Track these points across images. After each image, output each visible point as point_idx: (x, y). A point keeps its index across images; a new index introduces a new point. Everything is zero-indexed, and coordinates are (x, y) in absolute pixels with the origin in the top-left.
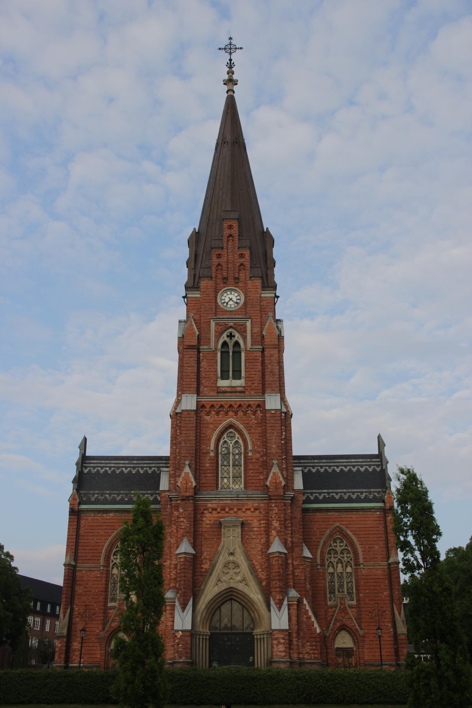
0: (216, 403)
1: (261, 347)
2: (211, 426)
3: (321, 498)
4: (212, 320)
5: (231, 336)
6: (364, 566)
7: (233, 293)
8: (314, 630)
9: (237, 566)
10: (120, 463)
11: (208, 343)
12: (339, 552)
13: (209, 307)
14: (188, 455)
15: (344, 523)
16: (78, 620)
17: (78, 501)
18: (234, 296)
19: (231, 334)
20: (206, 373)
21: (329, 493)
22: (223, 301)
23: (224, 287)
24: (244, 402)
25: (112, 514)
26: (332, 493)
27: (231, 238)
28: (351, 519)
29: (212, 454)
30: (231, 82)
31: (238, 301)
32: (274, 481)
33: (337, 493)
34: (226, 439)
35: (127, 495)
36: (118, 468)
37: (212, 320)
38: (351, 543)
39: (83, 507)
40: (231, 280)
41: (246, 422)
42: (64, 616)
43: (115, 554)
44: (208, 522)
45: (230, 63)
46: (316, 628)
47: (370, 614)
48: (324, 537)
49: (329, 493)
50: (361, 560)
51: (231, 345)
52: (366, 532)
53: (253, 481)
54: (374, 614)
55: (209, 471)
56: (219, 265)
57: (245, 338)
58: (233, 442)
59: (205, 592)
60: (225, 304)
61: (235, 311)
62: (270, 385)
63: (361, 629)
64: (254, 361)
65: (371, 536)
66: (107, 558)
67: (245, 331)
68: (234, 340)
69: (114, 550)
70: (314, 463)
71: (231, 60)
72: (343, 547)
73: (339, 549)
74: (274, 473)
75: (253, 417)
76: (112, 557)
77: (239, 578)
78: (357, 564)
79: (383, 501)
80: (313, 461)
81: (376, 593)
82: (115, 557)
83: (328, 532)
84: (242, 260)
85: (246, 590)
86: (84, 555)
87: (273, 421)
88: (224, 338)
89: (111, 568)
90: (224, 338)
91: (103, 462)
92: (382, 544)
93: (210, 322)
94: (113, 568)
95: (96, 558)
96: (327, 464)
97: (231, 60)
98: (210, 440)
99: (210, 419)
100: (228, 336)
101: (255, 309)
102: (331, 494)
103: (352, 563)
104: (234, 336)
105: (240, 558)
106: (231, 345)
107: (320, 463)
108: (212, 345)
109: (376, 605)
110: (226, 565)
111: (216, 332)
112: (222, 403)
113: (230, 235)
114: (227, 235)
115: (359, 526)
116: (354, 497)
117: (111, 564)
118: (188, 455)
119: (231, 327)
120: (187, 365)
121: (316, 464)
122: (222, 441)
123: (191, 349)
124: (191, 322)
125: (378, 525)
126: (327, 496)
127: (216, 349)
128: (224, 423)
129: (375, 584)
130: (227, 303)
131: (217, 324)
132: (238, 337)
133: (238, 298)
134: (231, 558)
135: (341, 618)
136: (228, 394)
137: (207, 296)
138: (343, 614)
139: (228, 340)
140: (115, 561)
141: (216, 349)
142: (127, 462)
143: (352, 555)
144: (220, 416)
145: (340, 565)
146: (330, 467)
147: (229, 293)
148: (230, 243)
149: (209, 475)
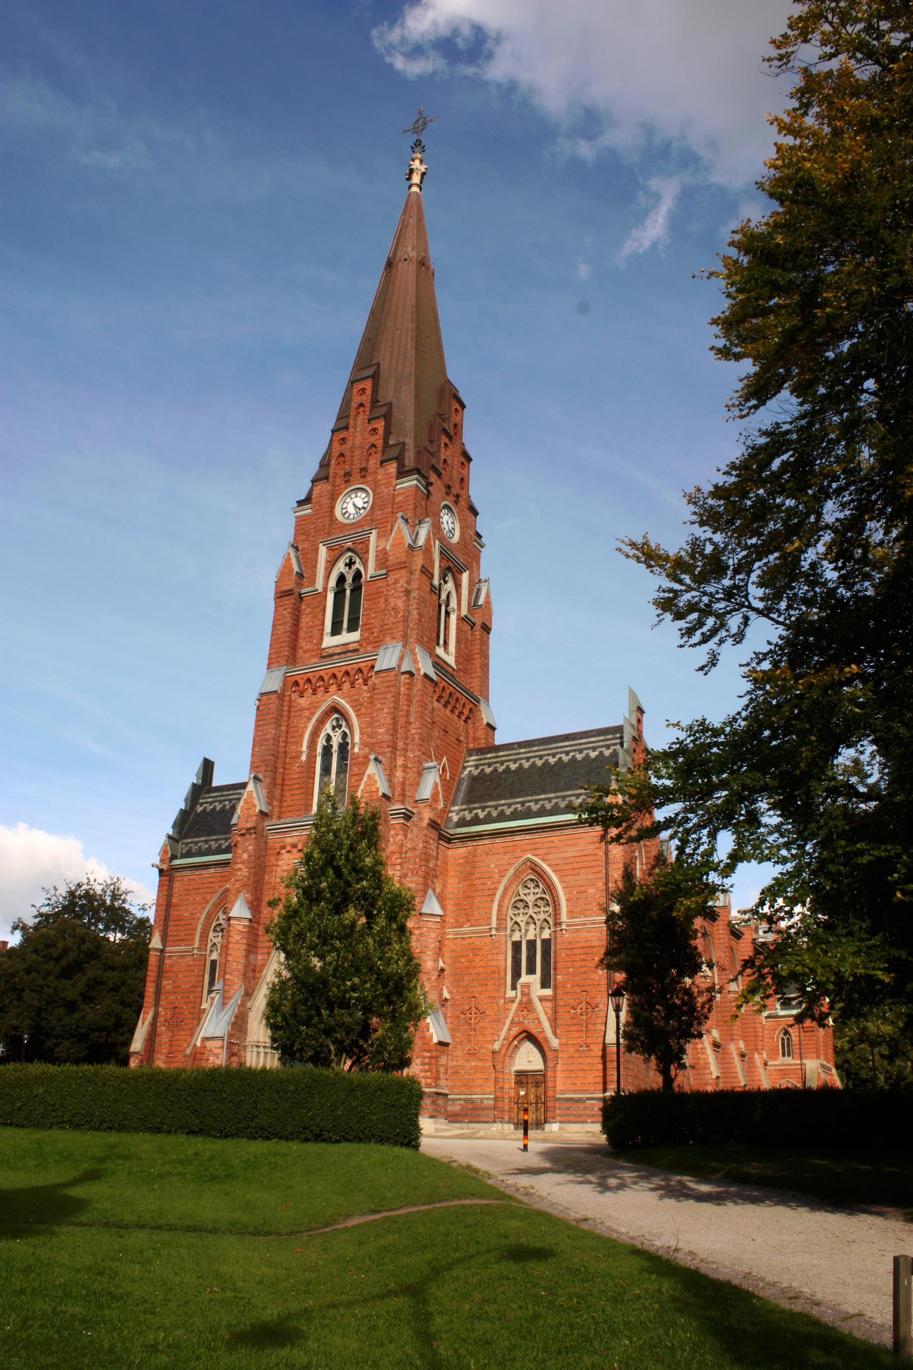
0: (313, 674)
3: (508, 812)
4: (321, 545)
6: (567, 926)
7: (359, 494)
8: (428, 1037)
11: (313, 582)
12: (530, 904)
14: (262, 764)
16: (164, 1028)
17: (169, 855)
18: (360, 500)
19: (351, 560)
22: (344, 511)
23: (346, 488)
24: (352, 666)
25: (212, 870)
26: (530, 801)
27: (362, 409)
28: (551, 844)
29: (304, 758)
32: (368, 788)
33: (536, 801)
34: (330, 732)
37: (321, 545)
38: (550, 888)
40: (356, 475)
42: (143, 1023)
43: (215, 930)
44: (285, 867)
46: (432, 1034)
47: (572, 1011)
48: (505, 881)
49: (523, 803)
50: (564, 917)
52: (575, 866)
54: (579, 1011)
55: (297, 786)
56: (342, 455)
61: (359, 522)
63: (555, 1034)
64: (376, 596)
66: (204, 936)
68: (354, 567)
69: (214, 924)
70: (520, 753)
72: (539, 896)
73: (530, 899)
74: (369, 776)
75: (365, 688)
78: (557, 923)
81: (585, 973)
83: (511, 871)
84: (373, 439)
86: (176, 933)
87: (382, 690)
88: (340, 567)
89: (208, 951)
93: (318, 548)
94: (211, 951)
96: (538, 754)
98: (302, 735)
100: (346, 565)
103: (551, 921)
104: (355, 563)
107: (528, 752)
108: (319, 586)
109: (584, 993)
111: (327, 561)
112: (322, 673)
113: (362, 405)
114: (356, 405)
116: (563, 805)
119: (349, 550)
121: (520, 756)
122: (323, 736)
123: (292, 597)
125: (596, 851)
126: (519, 809)
127: (325, 589)
128: (324, 707)
129: (584, 957)
131: (330, 549)
133: (366, 500)
135: (521, 1019)
136: (336, 657)
138: (525, 1013)
140: (214, 940)
141: (325, 589)
143: (550, 909)
144: (319, 695)
145: (532, 926)
146: (541, 757)
147: (353, 496)
148: (361, 417)
149: (296, 792)
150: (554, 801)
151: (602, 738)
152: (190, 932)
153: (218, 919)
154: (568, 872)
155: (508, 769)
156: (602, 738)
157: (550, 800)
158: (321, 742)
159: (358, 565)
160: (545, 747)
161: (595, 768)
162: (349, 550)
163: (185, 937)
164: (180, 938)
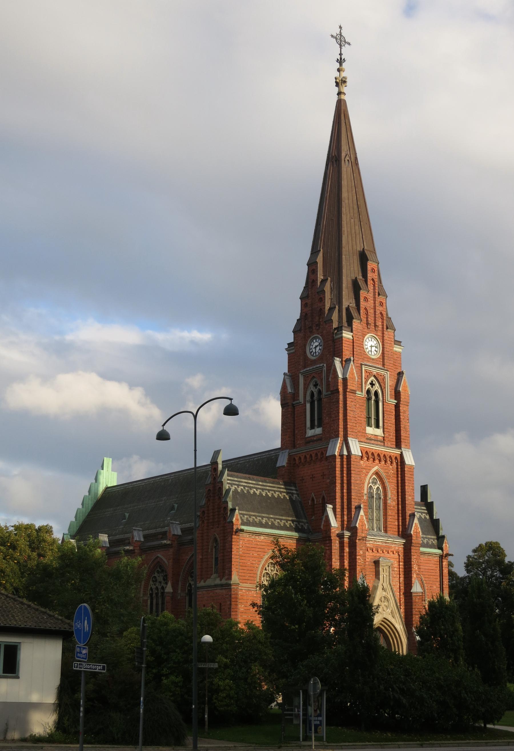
1: (396, 401)
2: (364, 471)
5: (372, 384)
13: (359, 351)
14: (357, 498)
19: (372, 381)
25: (262, 538)
30: (340, 83)
36: (251, 488)
39: (243, 527)
45: (341, 59)
58: (376, 487)
60: (370, 353)
65: (432, 577)
71: (341, 54)
75: (391, 467)
79: (440, 548)
85: (393, 621)
91: (236, 479)
92: (438, 584)
95: (252, 578)
97: (341, 54)
101: (390, 362)
104: (374, 385)
105: (390, 595)
118: (357, 498)
125: (436, 569)
130: (371, 351)
132: (377, 387)
134: (384, 593)
136: (373, 442)
142: (254, 482)
152: (252, 575)
153: (266, 569)
162: (375, 376)
163: (250, 578)
164: (246, 578)
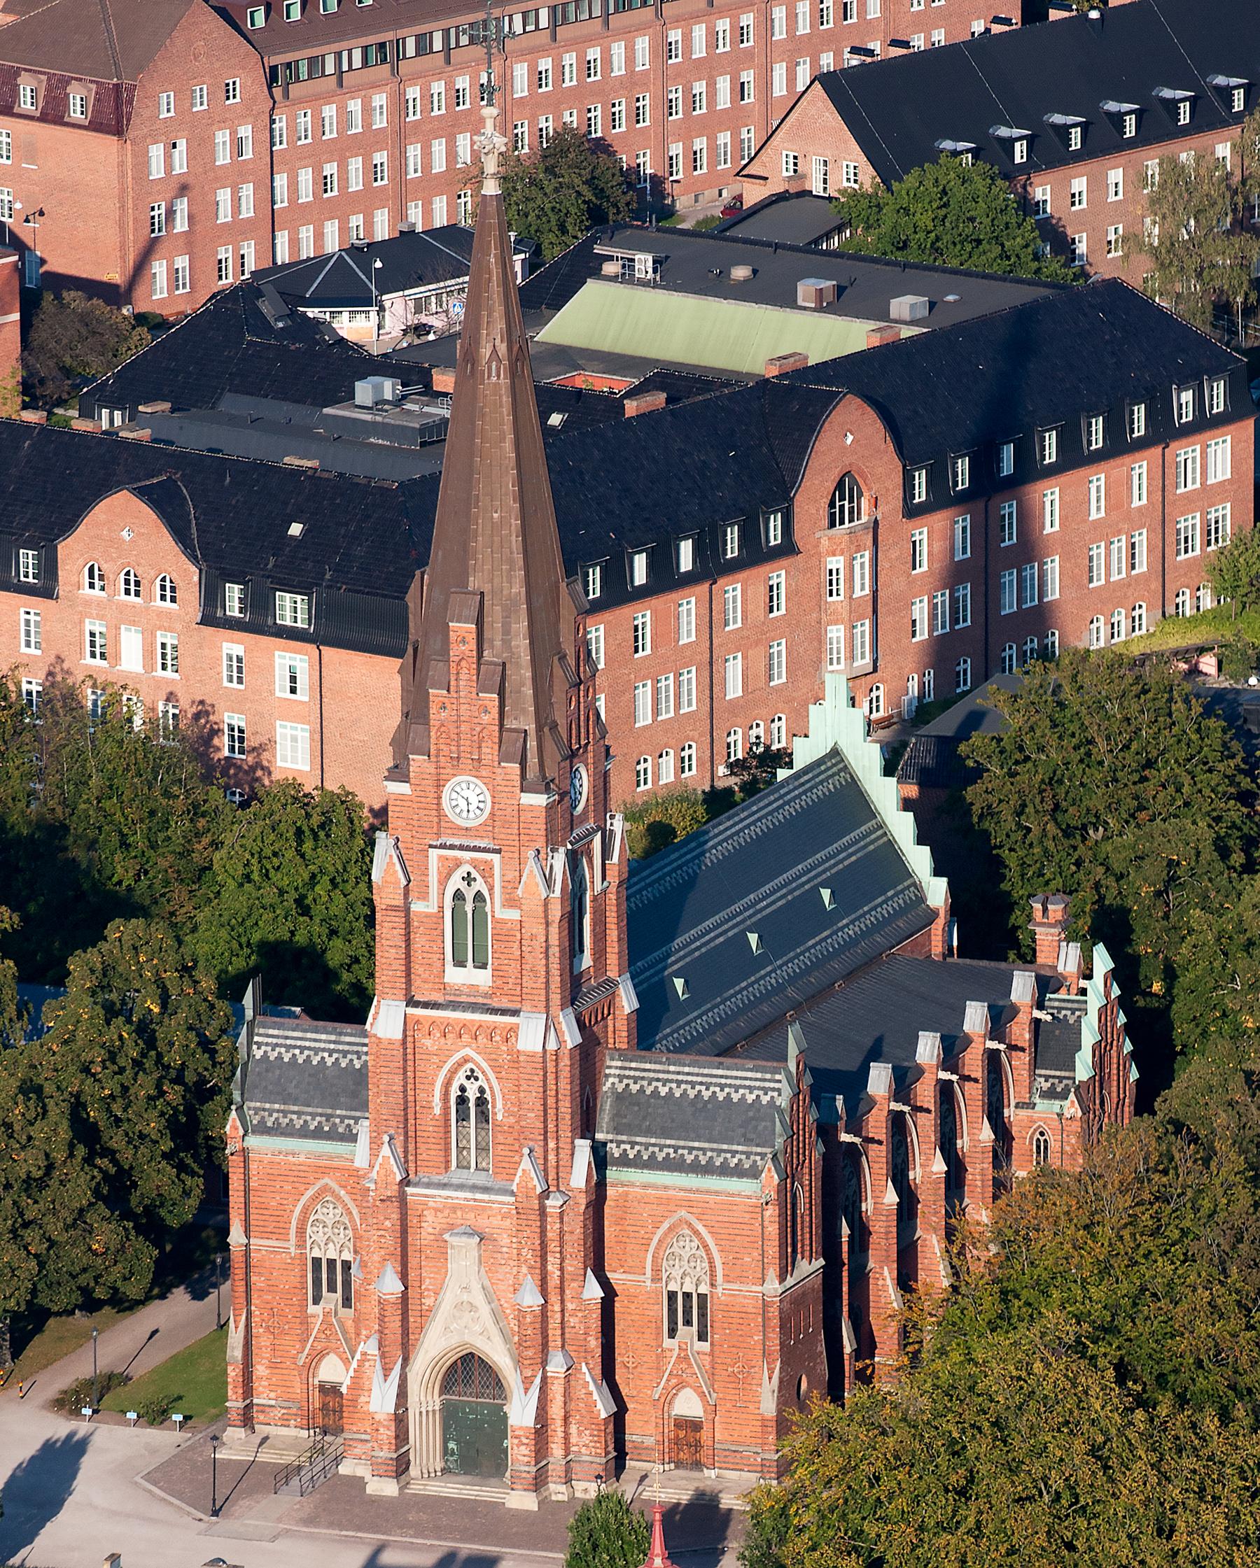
5: (468, 879)
9: (473, 1307)
10: (320, 1041)
13: (426, 818)
15: (694, 1210)
16: (261, 1330)
20: (425, 955)
21: (676, 1149)
22: (454, 803)
26: (684, 1148)
29: (437, 1111)
31: (481, 805)
35: (329, 1117)
40: (466, 763)
41: (494, 1056)
48: (660, 1232)
49: (676, 1149)
51: (469, 897)
52: (731, 1231)
53: (504, 1165)
57: (491, 889)
59: (425, 1345)
61: (476, 829)
62: (530, 997)
67: (492, 876)
76: (309, 1231)
77: (477, 1328)
80: (665, 1067)
82: (315, 1229)
86: (262, 1223)
87: (529, 1070)
88: (456, 883)
90: (456, 883)
99: (433, 1046)
102: (680, 1151)
105: (479, 1299)
106: (469, 897)
110: (459, 1306)
111: (439, 873)
115: (720, 1219)
117: (309, 1242)
120: (388, 943)
124: (391, 856)
128: (457, 1057)
137: (422, 794)
139: (462, 886)
144: (449, 1042)
150: (709, 1154)
151: (759, 1075)
154: (723, 1237)
155: (656, 1092)
156: (759, 1075)
157: (704, 1150)
158: (454, 1093)
159: (479, 885)
160: (696, 1070)
161: (752, 1119)
